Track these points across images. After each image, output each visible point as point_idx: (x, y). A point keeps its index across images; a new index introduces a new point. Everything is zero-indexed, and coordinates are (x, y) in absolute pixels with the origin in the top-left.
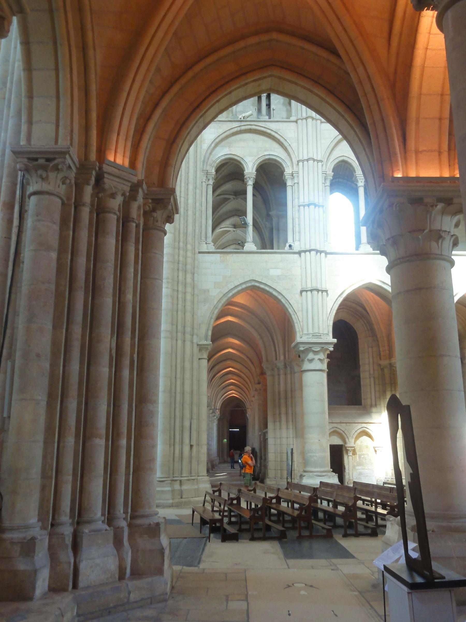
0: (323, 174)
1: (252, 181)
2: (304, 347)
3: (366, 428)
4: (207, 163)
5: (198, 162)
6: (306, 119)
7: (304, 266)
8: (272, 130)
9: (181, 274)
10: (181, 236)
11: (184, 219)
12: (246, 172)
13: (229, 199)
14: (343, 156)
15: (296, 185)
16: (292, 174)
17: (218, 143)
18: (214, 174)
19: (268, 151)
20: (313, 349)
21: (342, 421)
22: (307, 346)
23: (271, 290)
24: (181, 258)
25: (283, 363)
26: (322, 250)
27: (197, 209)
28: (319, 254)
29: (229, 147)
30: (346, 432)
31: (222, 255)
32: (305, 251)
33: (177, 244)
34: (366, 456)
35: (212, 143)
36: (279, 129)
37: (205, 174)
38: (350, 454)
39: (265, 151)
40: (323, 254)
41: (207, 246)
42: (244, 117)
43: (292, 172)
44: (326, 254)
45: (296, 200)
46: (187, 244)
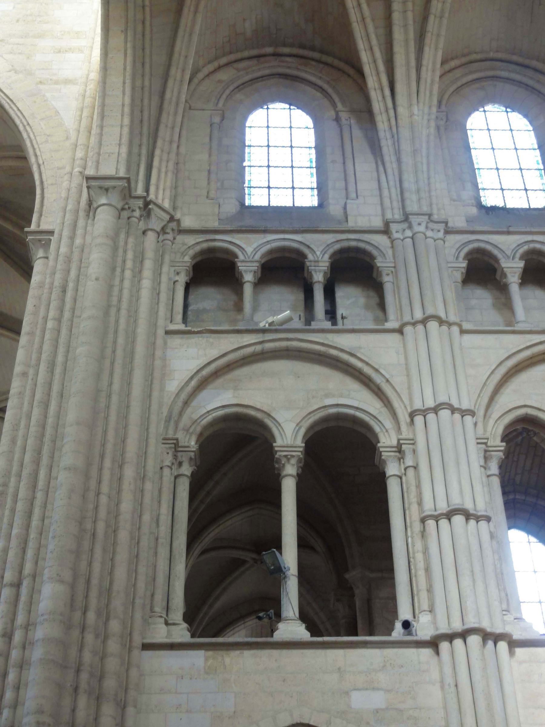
0: (478, 443)
1: (293, 465)
4: (177, 423)
5: (154, 418)
6: (424, 321)
7: (449, 680)
8: (342, 350)
9: (82, 701)
10: (94, 593)
11: (104, 550)
12: (279, 442)
13: (244, 562)
14: (525, 406)
15: (411, 472)
16: (399, 449)
18: (195, 449)
19: (334, 396)
24: (87, 656)
27: (145, 529)
28: (490, 643)
29: (236, 388)
31: (210, 653)
32: (450, 637)
33: (78, 615)
35: (192, 378)
36: (360, 348)
37: (170, 448)
39: (327, 396)
40: (503, 646)
41: (168, 632)
42: (271, 324)
43: (399, 440)
45: (414, 508)
46: (108, 619)
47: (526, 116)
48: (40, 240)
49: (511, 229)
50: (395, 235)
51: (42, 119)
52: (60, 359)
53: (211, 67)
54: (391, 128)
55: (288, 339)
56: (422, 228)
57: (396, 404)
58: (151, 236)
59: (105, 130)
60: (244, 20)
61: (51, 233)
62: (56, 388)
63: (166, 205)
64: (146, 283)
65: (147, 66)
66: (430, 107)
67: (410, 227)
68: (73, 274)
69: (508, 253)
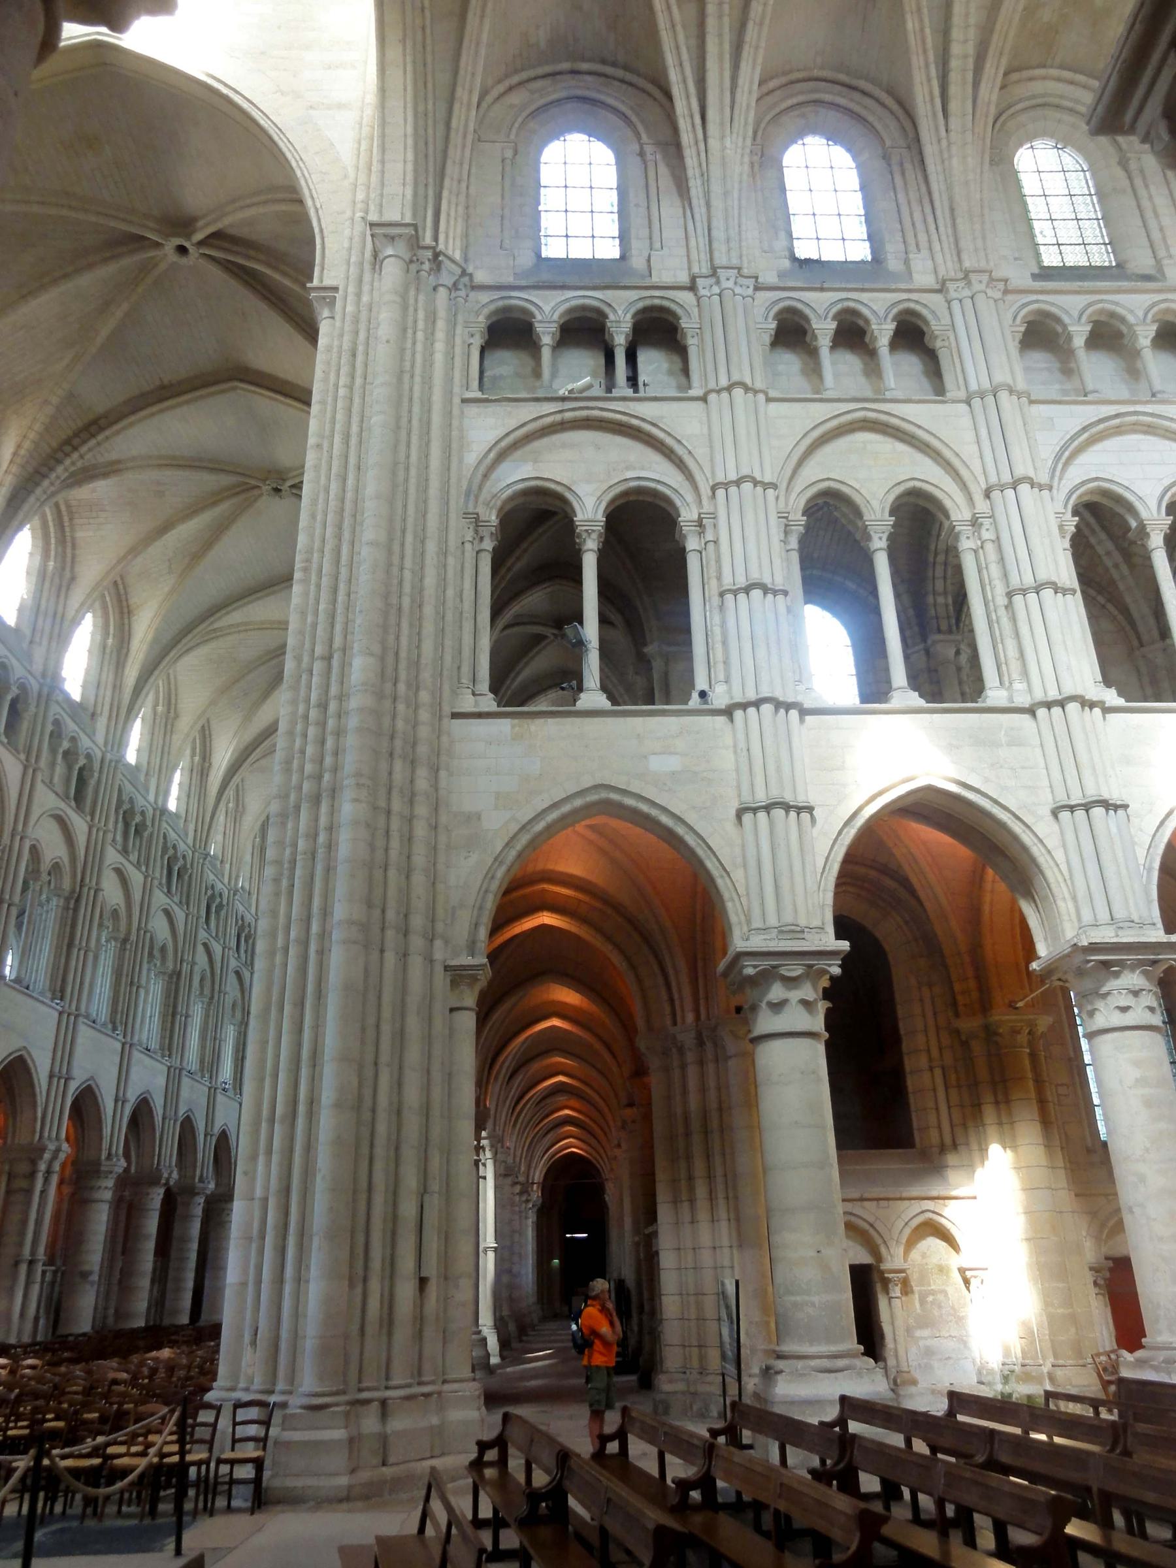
2: (755, 967)
3: (934, 1212)
4: (477, 497)
5: (453, 491)
6: (729, 389)
7: (742, 745)
8: (643, 420)
9: (398, 765)
10: (403, 665)
11: (411, 625)
12: (579, 517)
13: (544, 637)
14: (828, 479)
15: (711, 546)
16: (700, 523)
17: (506, 451)
19: (634, 469)
20: (783, 971)
21: (866, 1195)
22: (766, 963)
23: (654, 812)
24: (400, 724)
25: (693, 1034)
26: (790, 700)
27: (450, 604)
28: (782, 711)
29: (535, 461)
30: (878, 1225)
31: (516, 721)
32: (744, 706)
33: (388, 686)
34: (940, 1297)
35: (490, 450)
36: (662, 417)
38: (896, 1291)
39: (627, 468)
40: (794, 713)
41: (476, 701)
42: (571, 392)
44: (804, 712)
45: (714, 583)
46: (418, 689)
47: (849, 150)
48: (324, 298)
49: (826, 285)
50: (702, 292)
51: (317, 153)
52: (355, 428)
53: (501, 88)
54: (700, 165)
55: (588, 408)
56: (730, 284)
57: (698, 477)
58: (442, 292)
59: (387, 166)
60: (538, 27)
61: (336, 289)
62: (352, 460)
63: (457, 256)
64: (440, 346)
65: (430, 85)
66: (744, 139)
67: (718, 282)
68: (362, 335)
69: (821, 311)
